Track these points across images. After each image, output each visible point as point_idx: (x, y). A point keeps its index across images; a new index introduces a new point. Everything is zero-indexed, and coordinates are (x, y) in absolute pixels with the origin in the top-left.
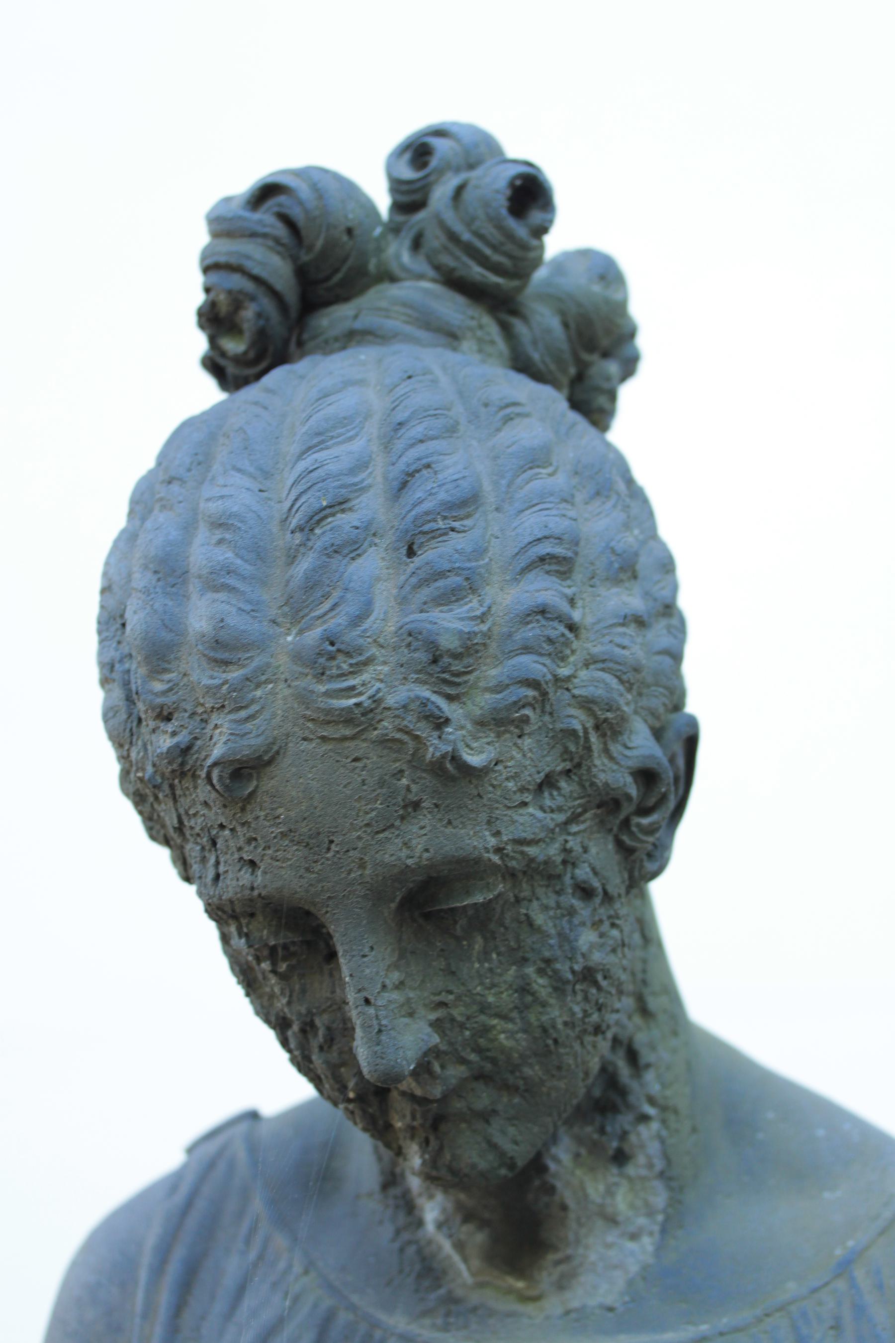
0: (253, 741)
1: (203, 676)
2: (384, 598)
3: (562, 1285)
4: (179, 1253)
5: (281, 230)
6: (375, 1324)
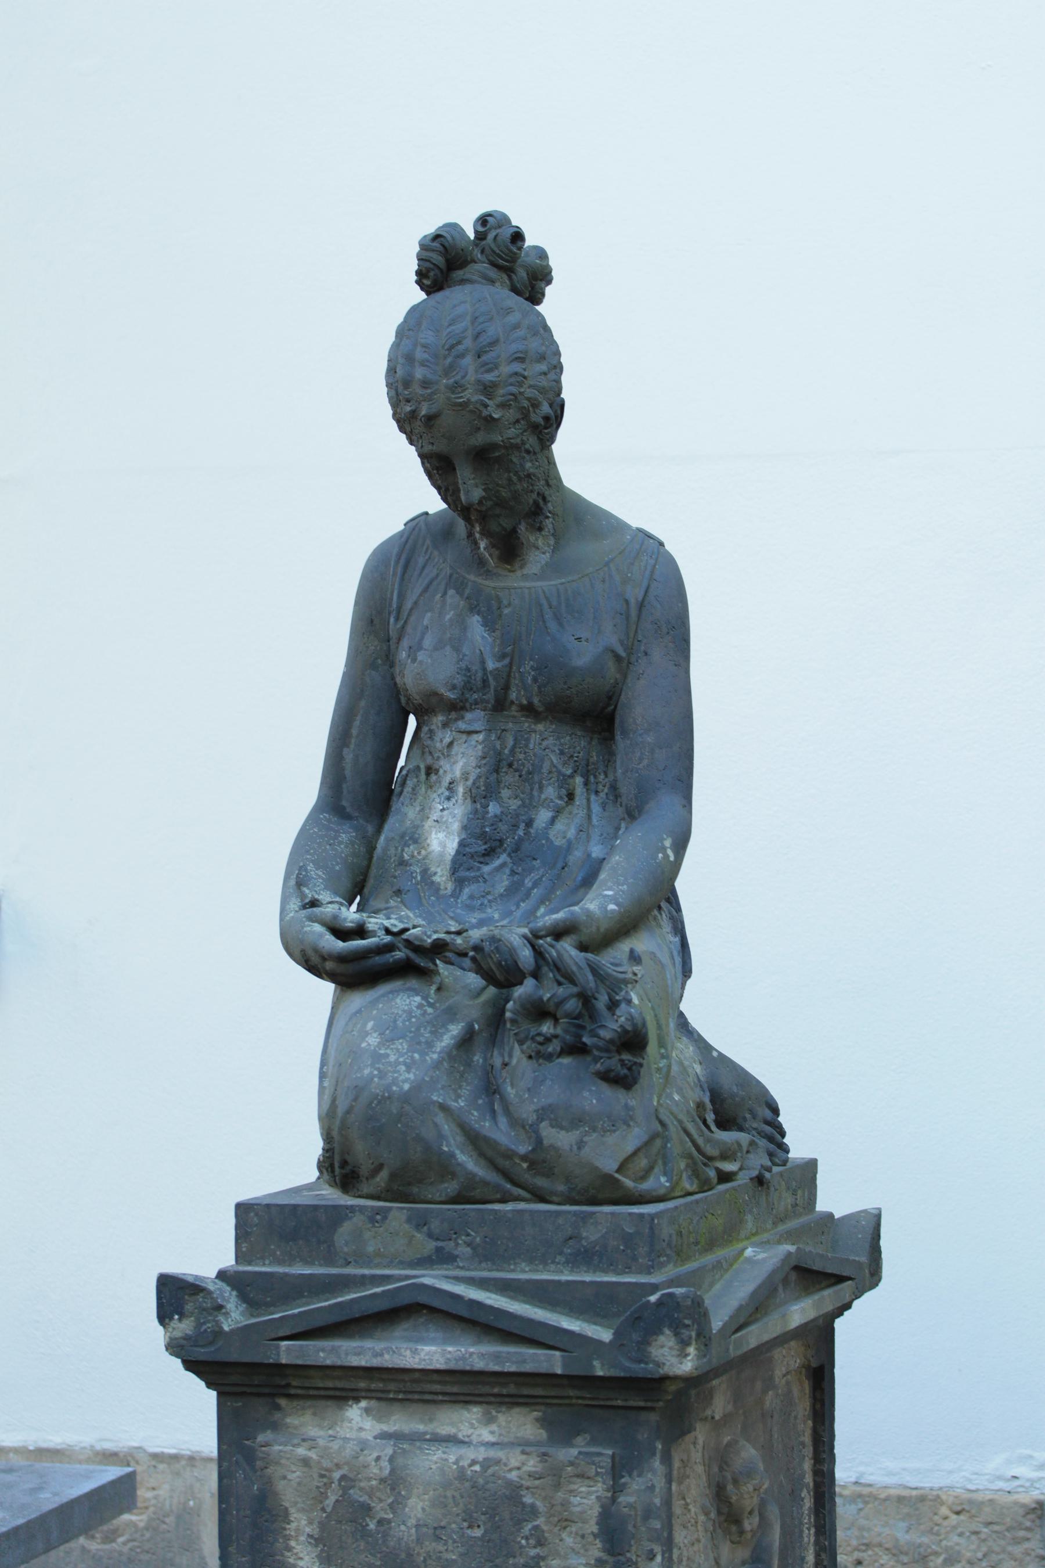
0: (434, 411)
1: (420, 391)
2: (471, 370)
3: (522, 567)
4: (404, 556)
5: (441, 249)
6: (465, 578)
